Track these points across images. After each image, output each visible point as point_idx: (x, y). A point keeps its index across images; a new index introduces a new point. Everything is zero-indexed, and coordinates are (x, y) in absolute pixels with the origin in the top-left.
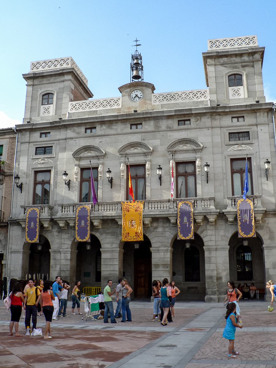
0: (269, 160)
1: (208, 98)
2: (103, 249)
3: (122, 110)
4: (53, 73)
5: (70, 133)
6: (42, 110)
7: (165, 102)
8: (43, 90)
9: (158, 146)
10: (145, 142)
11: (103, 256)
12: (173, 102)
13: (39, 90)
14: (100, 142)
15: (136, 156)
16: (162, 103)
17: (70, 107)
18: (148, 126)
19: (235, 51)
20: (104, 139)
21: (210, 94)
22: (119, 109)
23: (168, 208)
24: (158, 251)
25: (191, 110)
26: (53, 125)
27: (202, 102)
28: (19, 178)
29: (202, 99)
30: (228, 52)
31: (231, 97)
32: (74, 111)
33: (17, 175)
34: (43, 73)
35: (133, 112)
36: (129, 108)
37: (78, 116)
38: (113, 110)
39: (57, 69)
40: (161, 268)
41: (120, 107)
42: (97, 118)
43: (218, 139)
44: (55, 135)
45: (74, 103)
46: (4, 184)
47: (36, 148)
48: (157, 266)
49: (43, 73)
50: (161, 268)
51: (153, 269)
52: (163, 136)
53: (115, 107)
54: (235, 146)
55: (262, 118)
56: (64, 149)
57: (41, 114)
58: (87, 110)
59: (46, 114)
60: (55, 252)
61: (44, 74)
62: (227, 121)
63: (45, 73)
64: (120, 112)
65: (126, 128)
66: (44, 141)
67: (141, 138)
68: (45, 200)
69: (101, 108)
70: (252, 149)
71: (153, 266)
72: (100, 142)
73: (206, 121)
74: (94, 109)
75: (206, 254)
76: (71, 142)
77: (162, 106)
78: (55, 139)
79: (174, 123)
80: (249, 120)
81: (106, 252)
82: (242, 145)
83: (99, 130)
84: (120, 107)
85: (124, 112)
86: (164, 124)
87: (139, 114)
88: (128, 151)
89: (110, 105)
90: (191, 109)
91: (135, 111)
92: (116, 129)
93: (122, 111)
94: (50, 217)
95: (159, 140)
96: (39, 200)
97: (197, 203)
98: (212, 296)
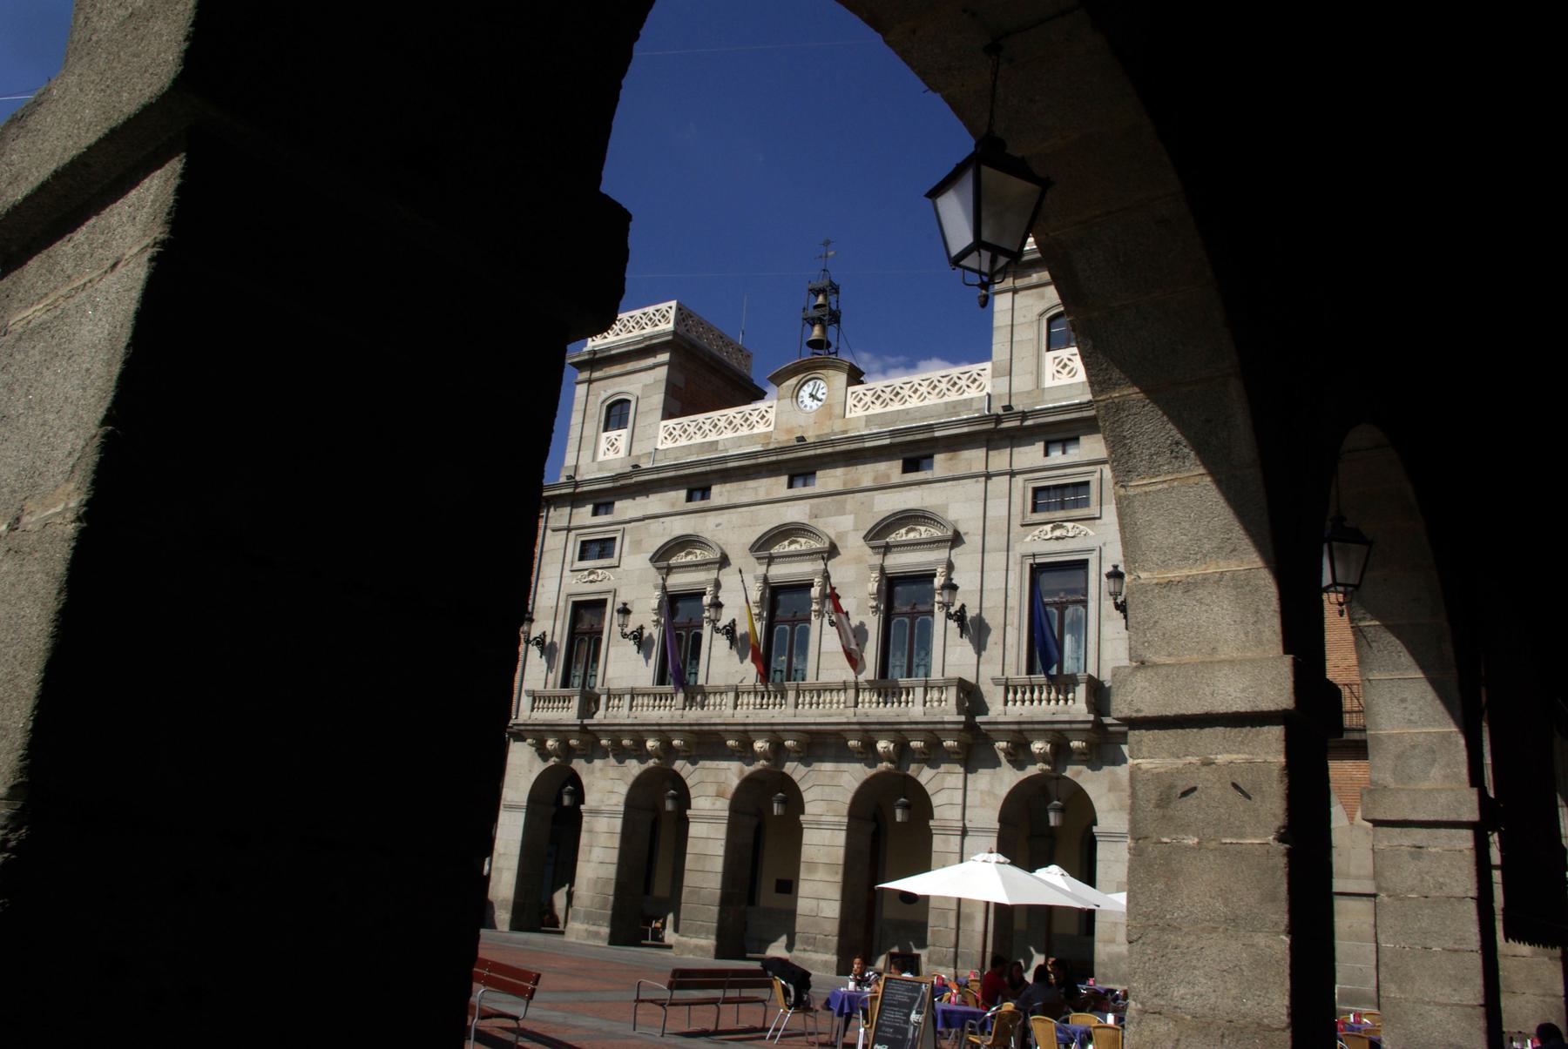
0: (1121, 569)
1: (988, 389)
2: (810, 818)
3: (774, 436)
4: (631, 348)
6: (603, 445)
7: (877, 409)
8: (610, 392)
9: (847, 533)
12: (896, 406)
13: (602, 392)
14: (717, 526)
15: (794, 562)
16: (867, 413)
17: (662, 434)
18: (829, 479)
20: (724, 517)
21: (993, 377)
22: (767, 435)
23: (842, 706)
25: (930, 427)
26: (618, 484)
27: (968, 403)
29: (972, 393)
31: (1048, 382)
32: (669, 444)
33: (625, 604)
34: (609, 349)
36: (789, 431)
37: (676, 459)
40: (821, 875)
41: (771, 428)
43: (998, 509)
44: (625, 508)
45: (671, 423)
48: (813, 865)
49: (611, 350)
52: (862, 503)
53: (760, 429)
54: (1048, 527)
56: (637, 545)
57: (601, 457)
58: (698, 439)
59: (611, 455)
61: (613, 352)
62: (1030, 455)
63: (614, 348)
65: (777, 486)
67: (811, 512)
68: (775, 672)
69: (729, 434)
70: (1091, 533)
71: (803, 867)
72: (717, 526)
73: (973, 458)
74: (712, 437)
76: (654, 525)
77: (869, 420)
82: (1065, 524)
84: (771, 428)
85: (778, 442)
86: (866, 474)
88: (776, 550)
89: (749, 425)
90: (932, 425)
91: (801, 439)
92: (756, 488)
93: (773, 440)
94: (579, 722)
95: (852, 516)
96: (579, 676)
97: (914, 694)
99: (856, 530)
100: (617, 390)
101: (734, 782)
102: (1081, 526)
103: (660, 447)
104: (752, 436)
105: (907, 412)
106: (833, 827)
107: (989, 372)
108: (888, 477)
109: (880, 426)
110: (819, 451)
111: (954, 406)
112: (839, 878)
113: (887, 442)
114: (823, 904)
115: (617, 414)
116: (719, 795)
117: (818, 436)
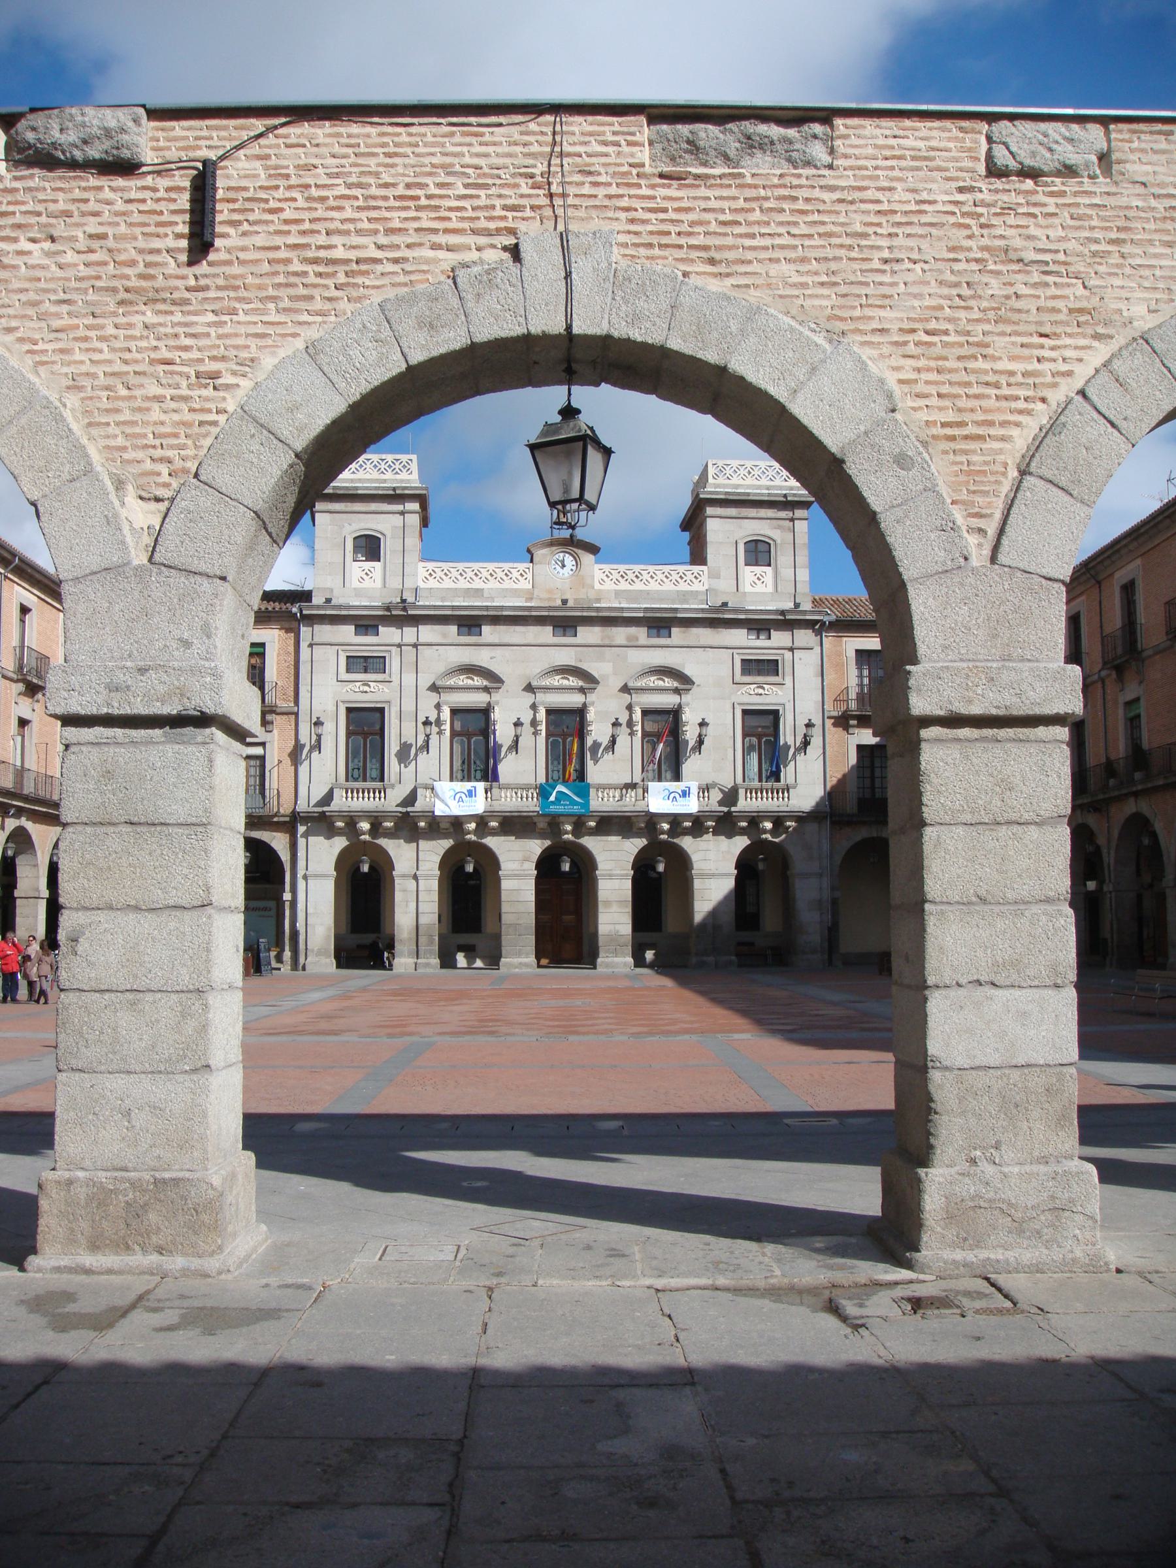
1: (706, 587)
5: (427, 633)
8: (355, 526)
10: (584, 666)
11: (505, 884)
18: (587, 634)
19: (762, 495)
24: (610, 877)
25: (676, 610)
27: (695, 594)
28: (322, 724)
30: (748, 494)
35: (559, 603)
36: (550, 591)
37: (443, 600)
38: (515, 593)
39: (385, 481)
40: (615, 908)
42: (487, 608)
45: (431, 565)
46: (275, 732)
47: (348, 657)
50: (615, 908)
51: (601, 909)
55: (804, 636)
59: (368, 583)
60: (404, 876)
61: (360, 492)
62: (739, 637)
64: (531, 599)
65: (546, 633)
66: (366, 644)
75: (697, 884)
77: (618, 594)
78: (388, 642)
79: (641, 633)
80: (780, 638)
81: (509, 877)
83: (489, 632)
86: (620, 634)
87: (572, 609)
91: (565, 602)
98: (705, 958)
99: (615, 674)
100: (363, 525)
101: (538, 851)
102: (774, 688)
103: (422, 585)
104: (516, 590)
105: (648, 592)
106: (622, 877)
107: (706, 572)
108: (637, 639)
109: (629, 600)
110: (585, 614)
111: (685, 596)
112: (629, 909)
113: (641, 615)
114: (617, 927)
115: (370, 547)
116: (526, 859)
117: (575, 600)
